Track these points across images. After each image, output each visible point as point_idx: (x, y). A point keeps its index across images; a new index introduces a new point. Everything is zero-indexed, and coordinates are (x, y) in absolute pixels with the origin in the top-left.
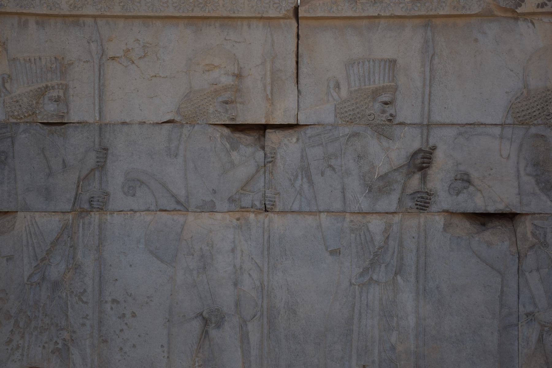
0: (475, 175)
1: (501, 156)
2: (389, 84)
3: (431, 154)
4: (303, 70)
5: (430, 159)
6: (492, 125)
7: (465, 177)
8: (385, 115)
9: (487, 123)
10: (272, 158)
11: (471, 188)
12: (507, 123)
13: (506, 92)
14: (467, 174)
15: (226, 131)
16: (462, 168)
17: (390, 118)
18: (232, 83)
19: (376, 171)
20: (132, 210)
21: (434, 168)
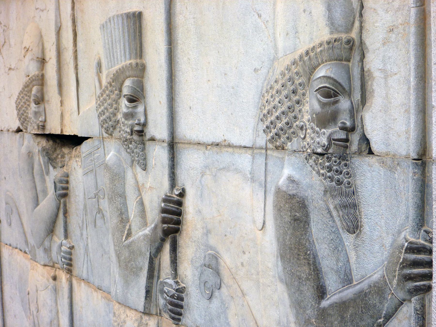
0: (227, 260)
1: (254, 222)
2: (128, 62)
3: (180, 204)
4: (80, 45)
5: (179, 214)
6: (240, 147)
7: (214, 262)
8: (130, 122)
9: (235, 145)
10: (64, 189)
11: (224, 290)
12: (258, 145)
13: (256, 70)
14: (216, 257)
15: (44, 142)
16: (212, 241)
17: (137, 128)
18: (37, 73)
19: (124, 227)
20: (10, 245)
21: (184, 233)
